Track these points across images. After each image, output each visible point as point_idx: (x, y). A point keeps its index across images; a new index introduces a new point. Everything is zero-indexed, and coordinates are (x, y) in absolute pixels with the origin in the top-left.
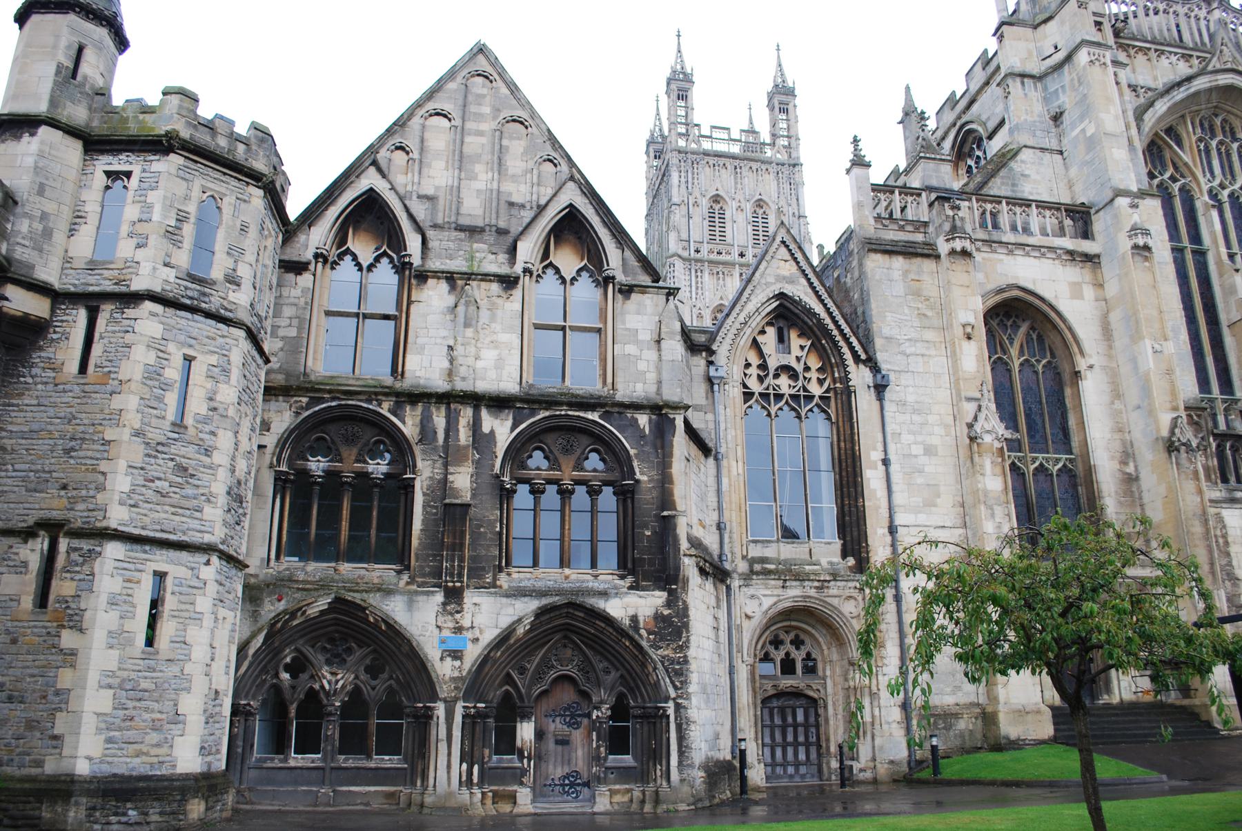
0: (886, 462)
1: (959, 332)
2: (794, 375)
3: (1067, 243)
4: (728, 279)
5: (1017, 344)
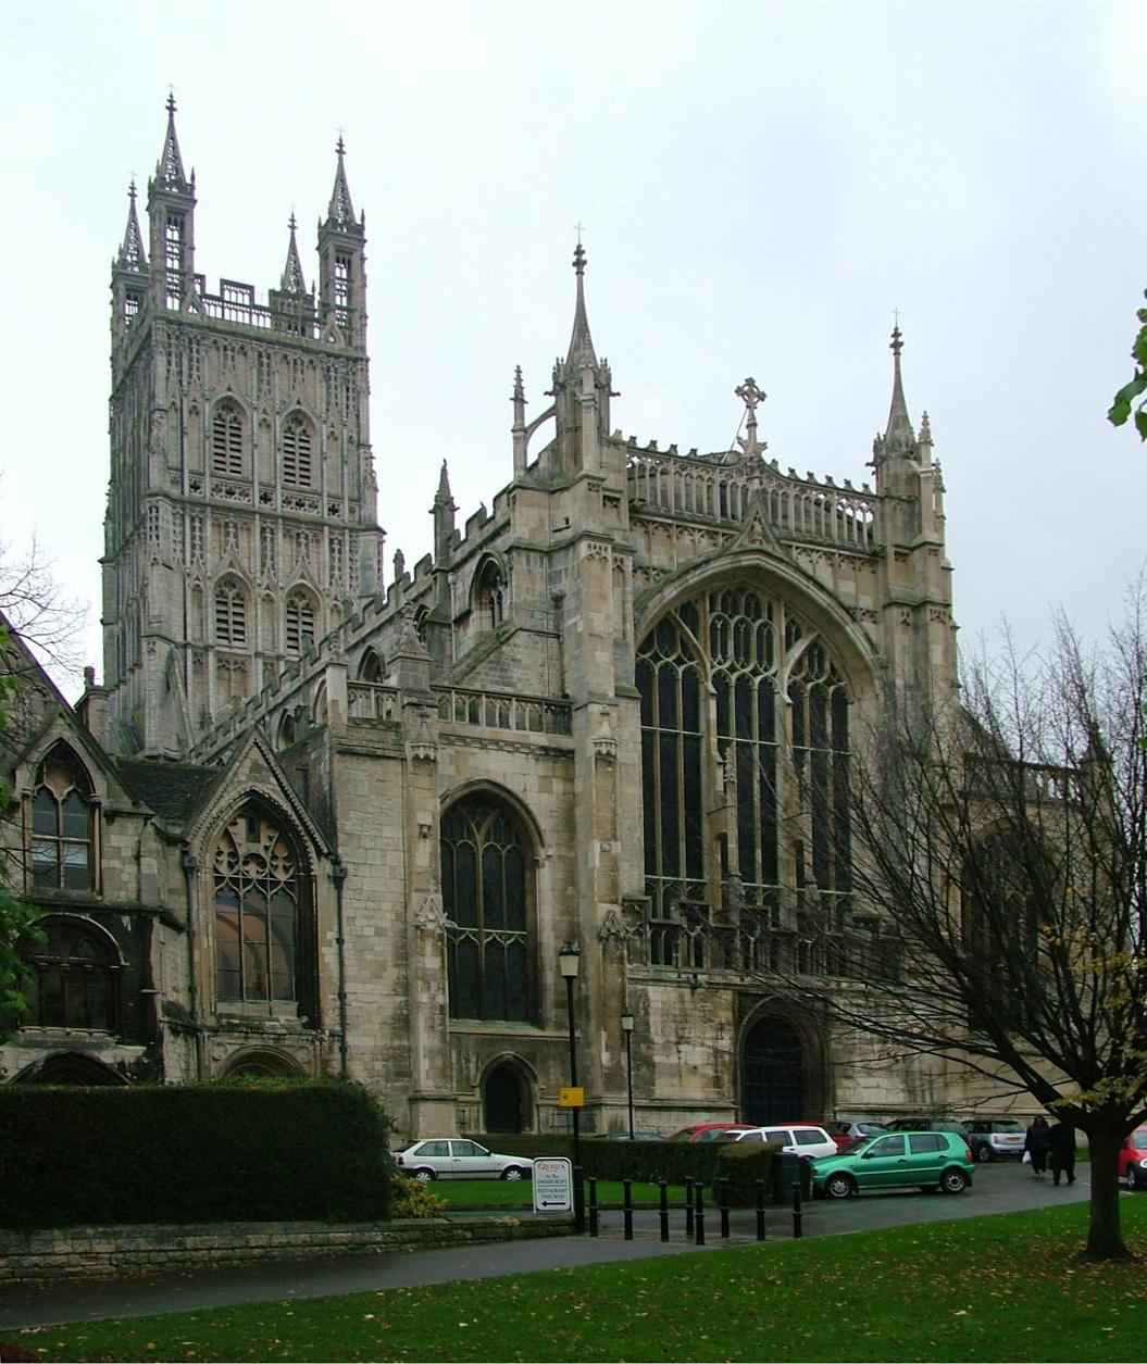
0: (340, 941)
1: (416, 831)
2: (262, 863)
3: (540, 739)
4: (243, 536)
5: (483, 831)
